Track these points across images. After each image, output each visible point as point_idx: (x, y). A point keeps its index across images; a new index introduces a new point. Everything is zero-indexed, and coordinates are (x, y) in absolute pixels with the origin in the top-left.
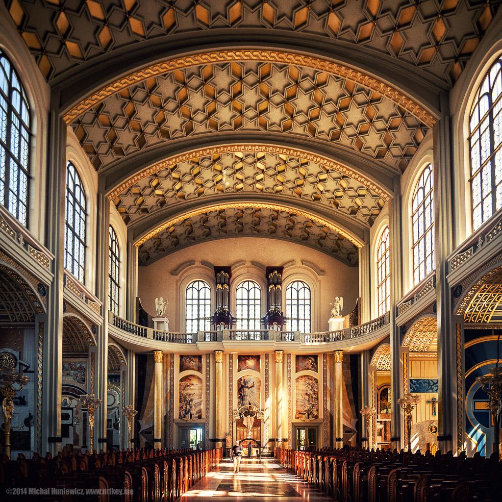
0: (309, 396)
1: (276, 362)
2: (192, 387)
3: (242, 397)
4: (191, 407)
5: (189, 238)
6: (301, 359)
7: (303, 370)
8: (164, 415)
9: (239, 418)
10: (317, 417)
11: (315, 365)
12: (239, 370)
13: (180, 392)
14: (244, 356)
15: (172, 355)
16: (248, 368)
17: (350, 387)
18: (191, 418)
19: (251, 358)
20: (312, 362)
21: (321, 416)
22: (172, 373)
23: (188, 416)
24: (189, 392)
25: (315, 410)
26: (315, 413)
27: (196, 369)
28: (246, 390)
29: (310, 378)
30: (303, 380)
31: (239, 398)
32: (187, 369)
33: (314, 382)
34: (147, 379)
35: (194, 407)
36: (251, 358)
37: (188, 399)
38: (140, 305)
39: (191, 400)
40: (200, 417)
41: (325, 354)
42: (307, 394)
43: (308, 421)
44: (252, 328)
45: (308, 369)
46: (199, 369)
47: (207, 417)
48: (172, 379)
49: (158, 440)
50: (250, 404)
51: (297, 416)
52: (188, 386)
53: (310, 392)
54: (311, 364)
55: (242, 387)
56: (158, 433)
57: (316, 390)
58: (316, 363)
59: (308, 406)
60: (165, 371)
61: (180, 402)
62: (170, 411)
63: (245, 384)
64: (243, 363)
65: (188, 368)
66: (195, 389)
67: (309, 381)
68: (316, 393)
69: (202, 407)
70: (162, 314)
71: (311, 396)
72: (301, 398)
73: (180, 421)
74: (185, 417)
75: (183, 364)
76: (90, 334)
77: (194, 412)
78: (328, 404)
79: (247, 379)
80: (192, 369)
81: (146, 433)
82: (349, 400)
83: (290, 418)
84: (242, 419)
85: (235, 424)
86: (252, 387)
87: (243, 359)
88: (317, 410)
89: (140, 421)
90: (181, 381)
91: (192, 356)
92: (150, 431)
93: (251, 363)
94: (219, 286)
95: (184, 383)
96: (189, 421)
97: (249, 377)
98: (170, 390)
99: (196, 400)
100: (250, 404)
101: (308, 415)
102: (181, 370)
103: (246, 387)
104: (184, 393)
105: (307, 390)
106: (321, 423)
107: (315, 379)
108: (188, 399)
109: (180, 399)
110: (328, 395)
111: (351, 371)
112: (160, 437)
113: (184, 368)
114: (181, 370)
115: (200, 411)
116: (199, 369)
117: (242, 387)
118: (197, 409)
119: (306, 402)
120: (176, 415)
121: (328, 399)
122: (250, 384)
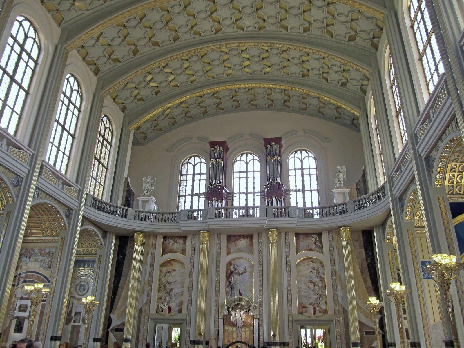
0: (314, 284)
1: (270, 242)
2: (173, 273)
3: (231, 286)
4: (171, 298)
5: (186, 117)
6: (301, 237)
7: (305, 250)
8: (140, 307)
9: (226, 313)
10: (325, 312)
11: (319, 245)
12: (228, 253)
13: (160, 280)
14: (234, 236)
15: (155, 235)
16: (240, 250)
17: (366, 271)
18: (169, 312)
19: (242, 239)
20: (316, 240)
21: (331, 311)
22: (153, 257)
23: (166, 308)
24: (170, 279)
25: (323, 302)
26: (324, 307)
27: (180, 251)
28: (236, 277)
29: (314, 260)
30: (306, 263)
31: (228, 286)
32: (170, 252)
33: (319, 265)
34: (125, 265)
35: (174, 298)
36: (242, 239)
37: (168, 288)
38: (128, 184)
39: (172, 290)
40: (180, 311)
41: (330, 231)
42: (311, 282)
43: (313, 317)
44: (250, 204)
45: (311, 249)
46: (183, 252)
47: (189, 311)
48: (152, 264)
49: (127, 341)
50: (241, 295)
51: (301, 310)
52: (169, 272)
53: (316, 279)
54: (315, 243)
55: (232, 272)
56: (129, 332)
57: (322, 276)
58: (321, 242)
59: (313, 297)
60: (144, 255)
61: (159, 291)
62: (146, 303)
63: (236, 270)
64: (233, 244)
65: (171, 251)
66: (177, 275)
67: (312, 265)
68: (322, 280)
69: (185, 299)
70: (149, 192)
71: (316, 284)
72: (303, 286)
73: (158, 316)
74: (162, 311)
75: (166, 247)
76: (62, 219)
77: (173, 305)
78: (339, 293)
79: (237, 262)
80: (176, 252)
81: (117, 330)
82: (367, 288)
83: (290, 312)
84: (230, 313)
85: (221, 321)
86: (243, 273)
87: (233, 239)
88: (326, 303)
89: (112, 315)
90: (163, 265)
91: (176, 237)
92: (120, 330)
93: (243, 243)
94: (213, 160)
95: (165, 269)
96: (168, 316)
97: (240, 260)
98: (149, 278)
99: (177, 290)
100: (241, 295)
101: (315, 309)
102: (163, 253)
103: (236, 274)
104: (164, 280)
105: (311, 277)
106: (332, 321)
107: (321, 262)
108: (168, 288)
109: (160, 288)
110: (338, 282)
111: (366, 251)
112: (130, 337)
113: (166, 250)
114: (163, 253)
115: (181, 303)
116: (183, 252)
117: (232, 272)
118: (178, 301)
119: (311, 293)
120: (153, 310)
121: (339, 287)
122: (241, 269)
